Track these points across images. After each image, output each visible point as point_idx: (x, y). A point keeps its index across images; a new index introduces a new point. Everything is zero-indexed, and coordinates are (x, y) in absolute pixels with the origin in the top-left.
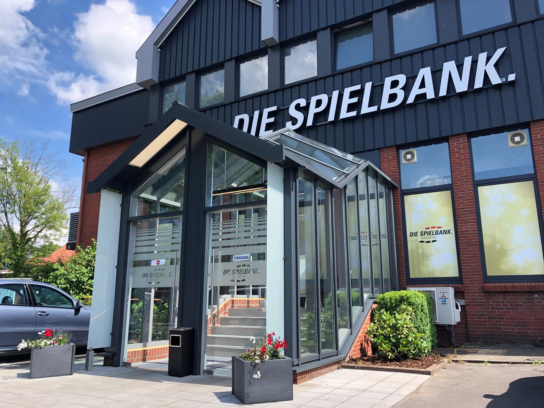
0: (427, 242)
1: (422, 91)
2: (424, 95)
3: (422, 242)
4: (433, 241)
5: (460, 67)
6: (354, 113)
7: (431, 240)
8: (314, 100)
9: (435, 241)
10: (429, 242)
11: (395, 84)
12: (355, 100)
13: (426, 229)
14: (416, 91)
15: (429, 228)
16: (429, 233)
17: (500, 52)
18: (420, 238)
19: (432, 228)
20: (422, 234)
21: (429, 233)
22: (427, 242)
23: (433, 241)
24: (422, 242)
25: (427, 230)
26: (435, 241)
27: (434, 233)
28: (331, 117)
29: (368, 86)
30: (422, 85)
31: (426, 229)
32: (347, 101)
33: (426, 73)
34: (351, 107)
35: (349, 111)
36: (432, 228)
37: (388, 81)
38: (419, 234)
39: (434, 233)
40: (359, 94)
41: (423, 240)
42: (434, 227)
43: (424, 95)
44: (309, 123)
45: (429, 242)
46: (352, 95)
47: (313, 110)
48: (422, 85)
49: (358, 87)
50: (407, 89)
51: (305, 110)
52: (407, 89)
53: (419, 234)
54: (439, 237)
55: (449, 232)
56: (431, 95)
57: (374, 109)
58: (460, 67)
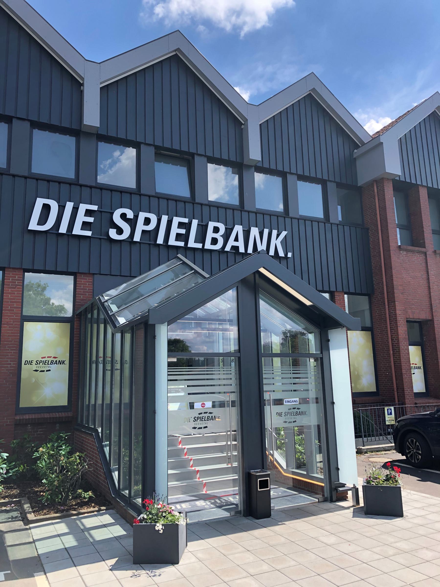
0: (41, 371)
1: (236, 244)
2: (238, 247)
3: (36, 371)
4: (47, 371)
5: (261, 234)
6: (182, 244)
7: (45, 370)
8: (142, 216)
9: (50, 370)
10: (44, 371)
11: (216, 230)
12: (183, 231)
13: (42, 358)
14: (231, 243)
15: (45, 357)
16: (44, 363)
17: (284, 233)
18: (34, 367)
19: (48, 357)
20: (37, 363)
21: (44, 363)
22: (41, 371)
23: (47, 371)
24: (36, 371)
25: (43, 360)
26: (50, 370)
27: (49, 363)
28: (160, 240)
29: (195, 223)
30: (236, 239)
31: (42, 358)
32: (175, 230)
33: (238, 229)
34: (179, 237)
35: (177, 240)
36: (48, 357)
37: (211, 225)
38: (34, 362)
39: (49, 363)
40: (187, 227)
41: (37, 369)
42: (50, 357)
43: (238, 247)
44: (137, 238)
45: (44, 371)
46: (181, 225)
47: (140, 227)
48: (236, 239)
49: (186, 220)
50: (226, 237)
51: (133, 223)
52: (226, 237)
53: (34, 362)
54: (53, 367)
55: (63, 362)
56: (242, 250)
57: (200, 246)
58: (261, 234)
